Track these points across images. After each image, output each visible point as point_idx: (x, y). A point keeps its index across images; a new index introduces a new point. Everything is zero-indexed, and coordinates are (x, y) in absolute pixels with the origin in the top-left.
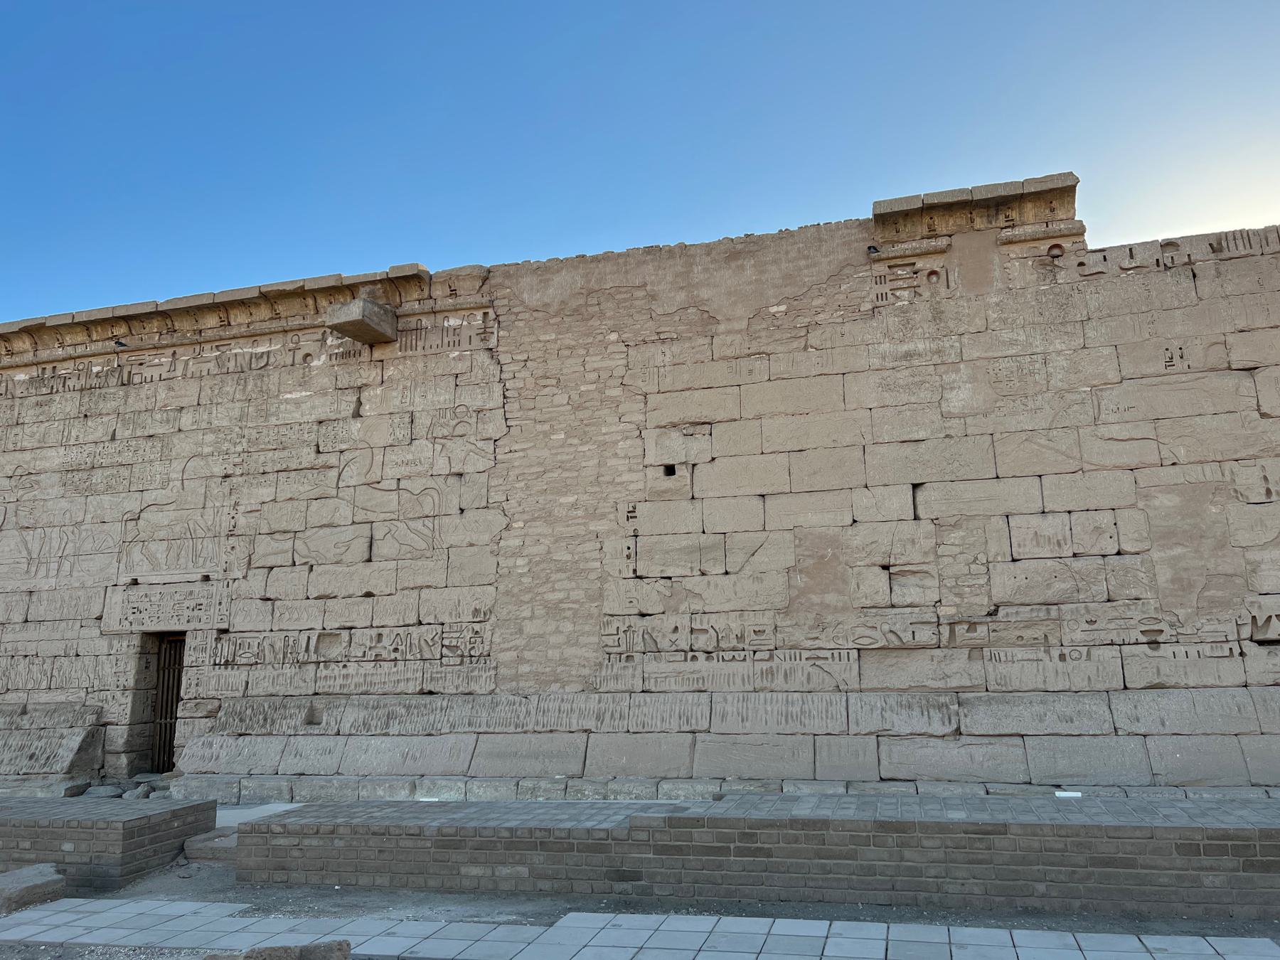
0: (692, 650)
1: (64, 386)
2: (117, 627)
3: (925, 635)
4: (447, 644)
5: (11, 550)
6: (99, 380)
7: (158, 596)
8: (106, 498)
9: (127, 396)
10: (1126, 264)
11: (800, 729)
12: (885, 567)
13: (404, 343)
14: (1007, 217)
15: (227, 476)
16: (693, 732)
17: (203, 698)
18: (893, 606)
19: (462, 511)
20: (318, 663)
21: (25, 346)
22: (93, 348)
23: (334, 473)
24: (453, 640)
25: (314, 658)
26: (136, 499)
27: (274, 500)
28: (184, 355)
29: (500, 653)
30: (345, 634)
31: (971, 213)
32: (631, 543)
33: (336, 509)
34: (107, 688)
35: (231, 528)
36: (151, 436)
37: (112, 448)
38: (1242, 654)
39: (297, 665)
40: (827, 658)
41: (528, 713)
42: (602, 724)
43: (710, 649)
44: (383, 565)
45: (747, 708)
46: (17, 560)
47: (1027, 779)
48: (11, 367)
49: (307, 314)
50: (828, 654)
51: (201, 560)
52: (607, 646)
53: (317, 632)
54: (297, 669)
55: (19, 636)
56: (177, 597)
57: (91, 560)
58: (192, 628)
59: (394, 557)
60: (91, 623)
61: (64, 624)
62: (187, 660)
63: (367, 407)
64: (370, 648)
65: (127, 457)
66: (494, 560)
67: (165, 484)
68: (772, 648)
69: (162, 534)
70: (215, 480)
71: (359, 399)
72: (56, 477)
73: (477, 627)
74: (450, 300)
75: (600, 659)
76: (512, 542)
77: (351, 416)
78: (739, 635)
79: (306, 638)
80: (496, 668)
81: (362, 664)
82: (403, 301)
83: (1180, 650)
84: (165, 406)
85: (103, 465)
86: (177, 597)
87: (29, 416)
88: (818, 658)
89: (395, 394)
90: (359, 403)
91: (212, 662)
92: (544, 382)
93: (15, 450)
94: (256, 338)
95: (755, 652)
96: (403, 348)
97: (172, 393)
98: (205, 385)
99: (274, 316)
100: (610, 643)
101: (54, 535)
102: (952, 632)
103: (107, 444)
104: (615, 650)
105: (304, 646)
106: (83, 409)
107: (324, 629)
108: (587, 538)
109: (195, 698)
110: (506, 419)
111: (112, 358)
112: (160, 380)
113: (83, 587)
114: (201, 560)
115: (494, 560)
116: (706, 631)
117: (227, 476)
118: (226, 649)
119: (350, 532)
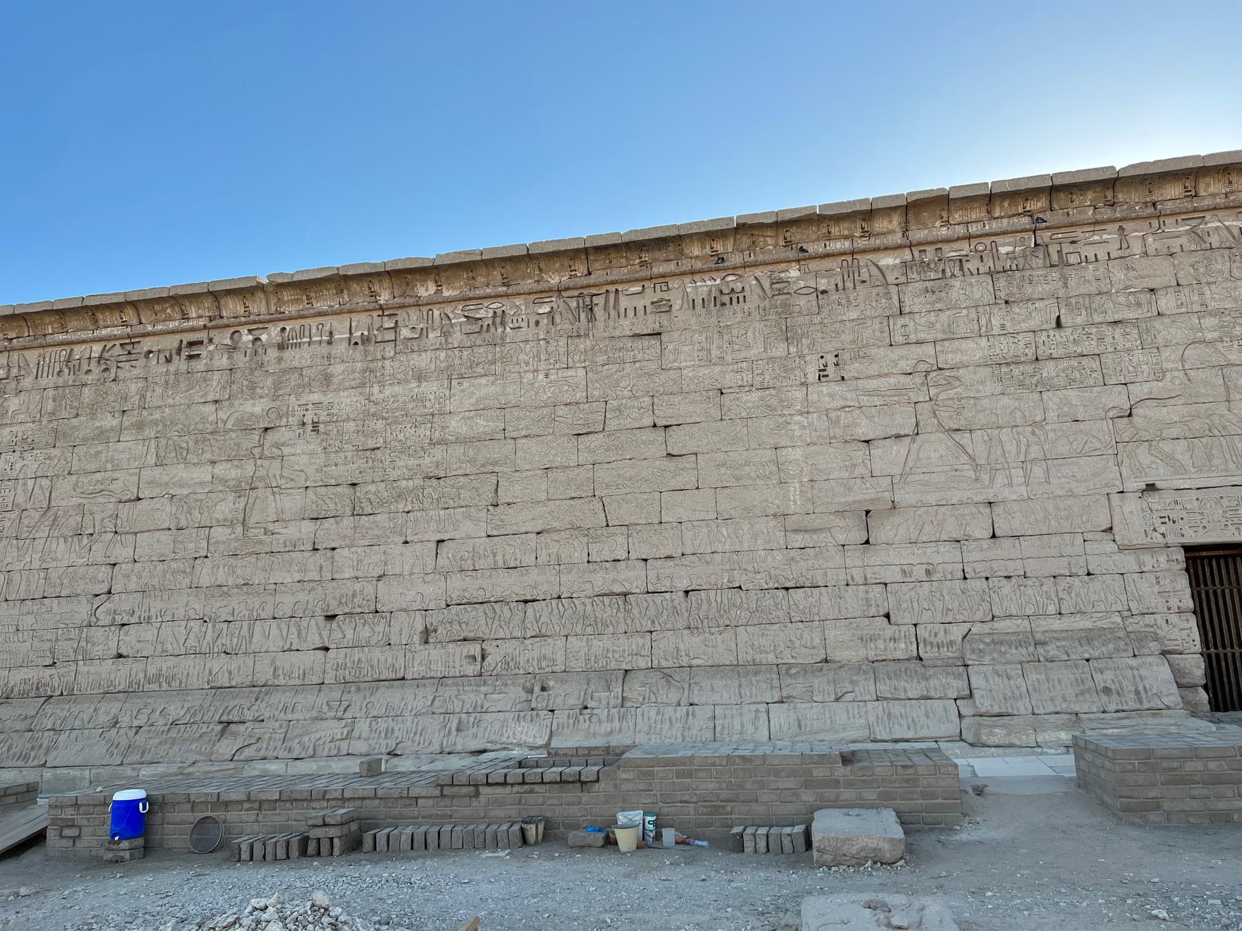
1: (961, 268)
2: (1141, 540)
5: (942, 456)
6: (1015, 262)
7: (1196, 504)
8: (1072, 394)
21: (890, 227)
22: (995, 226)
26: (1120, 393)
28: (1135, 232)
34: (1151, 610)
37: (1058, 336)
46: (956, 467)
48: (876, 250)
56: (1225, 502)
57: (1075, 464)
61: (1055, 540)
67: (1160, 374)
69: (1174, 432)
72: (984, 372)
84: (1127, 288)
85: (1054, 356)
97: (1132, 273)
98: (1180, 263)
101: (1004, 438)
103: (1052, 333)
111: (1026, 237)
112: (1109, 259)
113: (1071, 494)
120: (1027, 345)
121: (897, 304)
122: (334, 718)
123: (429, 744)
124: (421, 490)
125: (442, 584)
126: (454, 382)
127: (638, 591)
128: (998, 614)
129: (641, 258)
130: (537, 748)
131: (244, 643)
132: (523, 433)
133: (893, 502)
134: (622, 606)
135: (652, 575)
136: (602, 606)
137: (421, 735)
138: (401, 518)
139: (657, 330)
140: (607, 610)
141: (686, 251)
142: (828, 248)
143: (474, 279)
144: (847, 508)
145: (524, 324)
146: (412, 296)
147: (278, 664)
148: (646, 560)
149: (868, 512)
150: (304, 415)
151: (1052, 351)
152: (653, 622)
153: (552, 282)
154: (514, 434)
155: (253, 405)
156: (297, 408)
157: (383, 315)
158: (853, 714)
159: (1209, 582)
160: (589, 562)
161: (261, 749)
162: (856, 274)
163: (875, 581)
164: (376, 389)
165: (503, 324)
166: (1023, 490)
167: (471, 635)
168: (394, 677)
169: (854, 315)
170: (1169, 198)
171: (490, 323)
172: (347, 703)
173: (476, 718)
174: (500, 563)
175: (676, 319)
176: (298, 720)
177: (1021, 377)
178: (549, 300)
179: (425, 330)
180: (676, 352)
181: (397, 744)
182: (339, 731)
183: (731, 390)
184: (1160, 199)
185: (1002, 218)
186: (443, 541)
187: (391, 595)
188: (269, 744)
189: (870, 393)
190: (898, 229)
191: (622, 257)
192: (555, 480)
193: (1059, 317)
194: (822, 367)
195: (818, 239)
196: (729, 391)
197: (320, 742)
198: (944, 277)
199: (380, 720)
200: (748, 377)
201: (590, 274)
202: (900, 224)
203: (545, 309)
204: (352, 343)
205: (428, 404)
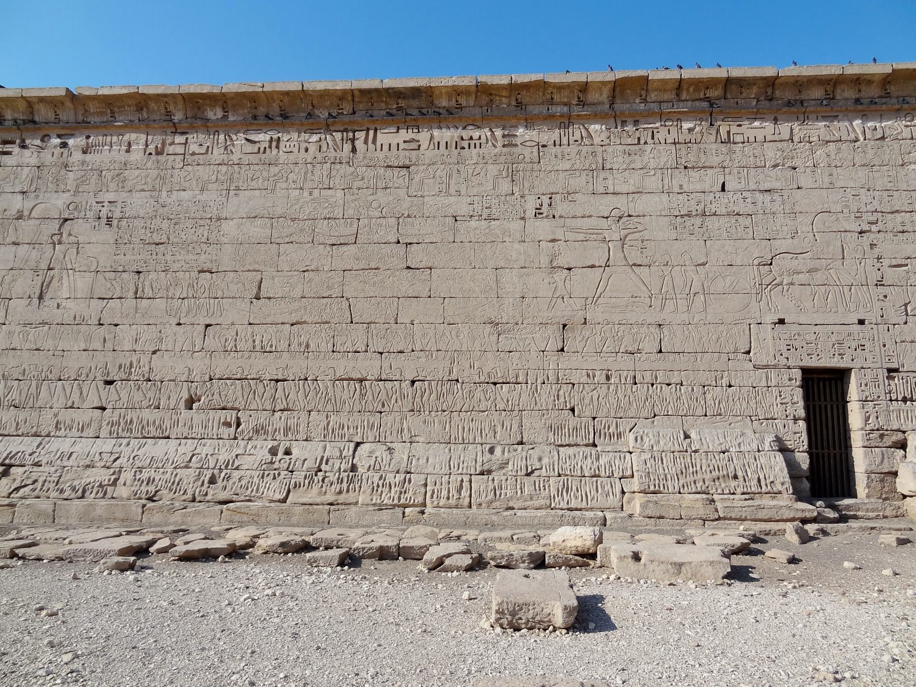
1: (653, 138)
9: (731, 152)
15: (861, 233)
35: (880, 279)
36: (770, 191)
55: (655, 366)
58: (859, 366)
60: (741, 356)
65: (742, 208)
86: (834, 338)
87: (617, 160)
91: (888, 398)
93: (607, 193)
94: (865, 113)
99: (883, 95)
103: (717, 195)
106: (683, 161)
109: (878, 430)
111: (705, 118)
114: (853, 307)
120: (698, 203)
121: (601, 161)
122: (104, 467)
123: (184, 494)
124: (196, 281)
125: (207, 361)
126: (232, 193)
127: (373, 378)
128: (658, 413)
129: (398, 104)
130: (275, 501)
131: (32, 398)
132: (287, 240)
133: (585, 319)
134: (358, 390)
135: (386, 365)
136: (342, 389)
137: (178, 484)
138: (176, 303)
139: (407, 163)
140: (346, 392)
141: (436, 102)
142: (550, 111)
143: (256, 108)
144: (549, 321)
145: (296, 150)
146: (202, 119)
147: (60, 418)
148: (381, 353)
149: (565, 326)
150: (100, 211)
151: (716, 209)
152: (383, 406)
153: (322, 116)
154: (278, 241)
155: (58, 199)
156: (94, 204)
157: (174, 133)
158: (539, 487)
159: (816, 398)
160: (333, 351)
161: (36, 489)
162: (571, 134)
163: (565, 382)
164: (164, 194)
165: (277, 147)
166: (685, 317)
167: (229, 405)
168: (161, 435)
169: (567, 165)
171: (267, 146)
172: (117, 455)
173: (227, 474)
174: (258, 348)
175: (423, 156)
176: (72, 467)
177: (692, 228)
178: (318, 131)
179: (210, 149)
180: (422, 182)
181: (156, 492)
182: (107, 478)
183: (464, 218)
185: (687, 101)
186: (210, 325)
187: (163, 366)
188: (43, 485)
189: (573, 230)
190: (606, 101)
191: (382, 102)
192: (310, 281)
193: (724, 183)
194: (539, 207)
195: (543, 103)
196: (461, 218)
197: (90, 486)
198: (639, 143)
199: (144, 470)
200: (478, 207)
201: (354, 113)
202: (608, 97)
203: (315, 138)
204: (147, 153)
205: (207, 209)
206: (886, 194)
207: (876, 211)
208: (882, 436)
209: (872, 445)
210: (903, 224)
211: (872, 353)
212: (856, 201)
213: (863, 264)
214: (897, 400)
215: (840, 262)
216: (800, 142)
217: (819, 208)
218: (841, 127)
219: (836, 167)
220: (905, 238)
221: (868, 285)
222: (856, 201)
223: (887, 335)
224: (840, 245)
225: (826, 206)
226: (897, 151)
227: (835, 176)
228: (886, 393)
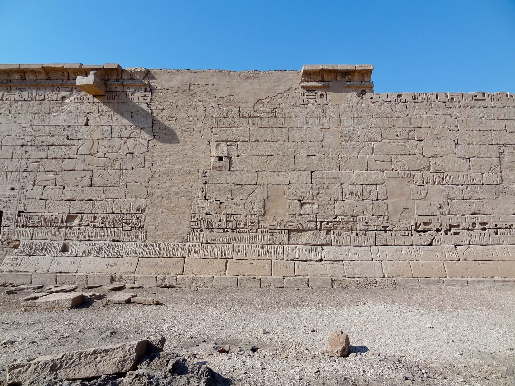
0: (226, 228)
3: (312, 225)
4: (125, 222)
10: (386, 100)
11: (266, 258)
12: (300, 200)
13: (109, 97)
14: (348, 77)
15: (23, 146)
16: (226, 258)
17: (12, 240)
18: (301, 215)
19: (133, 168)
20: (66, 227)
23: (75, 148)
24: (128, 220)
25: (65, 225)
27: (47, 158)
29: (148, 226)
30: (79, 215)
31: (337, 74)
32: (204, 185)
33: (76, 164)
35: (26, 168)
38: (412, 235)
39: (57, 228)
40: (277, 233)
41: (160, 250)
42: (190, 255)
43: (233, 228)
44: (97, 188)
45: (247, 250)
47: (344, 275)
49: (64, 79)
50: (277, 231)
51: (10, 181)
52: (192, 225)
53: (66, 214)
54: (57, 230)
59: (102, 185)
62: (3, 223)
63: (91, 122)
64: (91, 222)
66: (146, 189)
68: (257, 228)
70: (17, 146)
71: (87, 118)
73: (138, 216)
74: (130, 81)
75: (190, 230)
76: (154, 182)
77: (84, 125)
78: (245, 223)
79: (61, 216)
80: (147, 232)
81: (87, 228)
82: (109, 79)
83: (393, 233)
88: (274, 233)
89: (104, 117)
90: (88, 120)
91: (16, 225)
92: (170, 119)
94: (39, 87)
95: (250, 230)
96: (109, 99)
99: (48, 78)
100: (194, 224)
102: (321, 224)
104: (196, 227)
105: (60, 220)
107: (70, 213)
108: (185, 183)
109: (8, 240)
110: (153, 133)
115: (145, 190)
116: (232, 221)
117: (23, 146)
118: (22, 220)
119: (83, 173)
170: (15, 79)
184: (12, 79)
206: (38, 127)
207: (32, 136)
208: (9, 243)
209: (3, 247)
210: (42, 142)
211: (13, 204)
212: (24, 130)
213: (20, 161)
214: (20, 226)
215: (10, 160)
216: (6, 101)
217: (6, 134)
218: (25, 95)
219: (19, 113)
220: (42, 149)
221: (20, 171)
222: (24, 130)
223: (22, 195)
224: (12, 151)
225: (10, 132)
226: (48, 106)
227: (17, 118)
228: (15, 223)
